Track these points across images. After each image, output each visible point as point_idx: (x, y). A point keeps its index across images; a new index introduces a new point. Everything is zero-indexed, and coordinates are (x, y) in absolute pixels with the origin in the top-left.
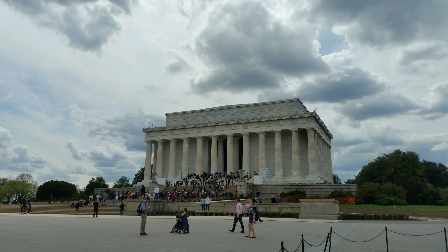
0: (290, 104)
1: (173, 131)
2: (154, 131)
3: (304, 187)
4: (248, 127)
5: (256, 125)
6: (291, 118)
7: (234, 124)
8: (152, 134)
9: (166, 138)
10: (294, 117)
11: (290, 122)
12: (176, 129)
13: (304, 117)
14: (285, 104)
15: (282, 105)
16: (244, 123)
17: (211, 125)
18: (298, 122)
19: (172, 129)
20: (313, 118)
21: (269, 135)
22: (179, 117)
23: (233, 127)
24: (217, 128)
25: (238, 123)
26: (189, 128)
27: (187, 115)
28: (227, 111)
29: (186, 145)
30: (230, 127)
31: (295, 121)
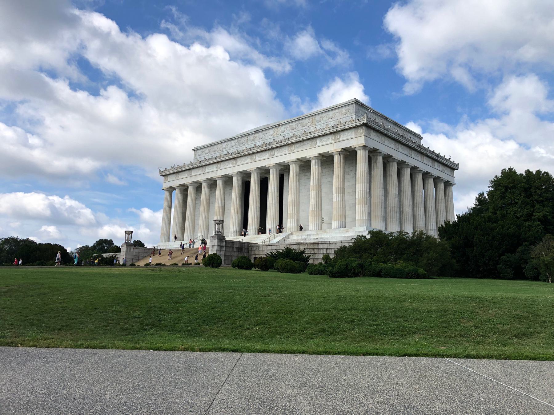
0: (343, 110)
1: (190, 172)
3: (316, 247)
4: (276, 154)
5: (286, 150)
6: (331, 133)
7: (259, 152)
8: (171, 178)
10: (334, 130)
11: (330, 139)
13: (350, 128)
14: (336, 111)
15: (331, 114)
16: (270, 149)
17: (232, 157)
18: (341, 139)
20: (364, 127)
21: (305, 165)
22: (207, 150)
24: (240, 161)
25: (263, 151)
26: (207, 165)
27: (215, 147)
29: (205, 190)
30: (254, 157)
31: (337, 136)
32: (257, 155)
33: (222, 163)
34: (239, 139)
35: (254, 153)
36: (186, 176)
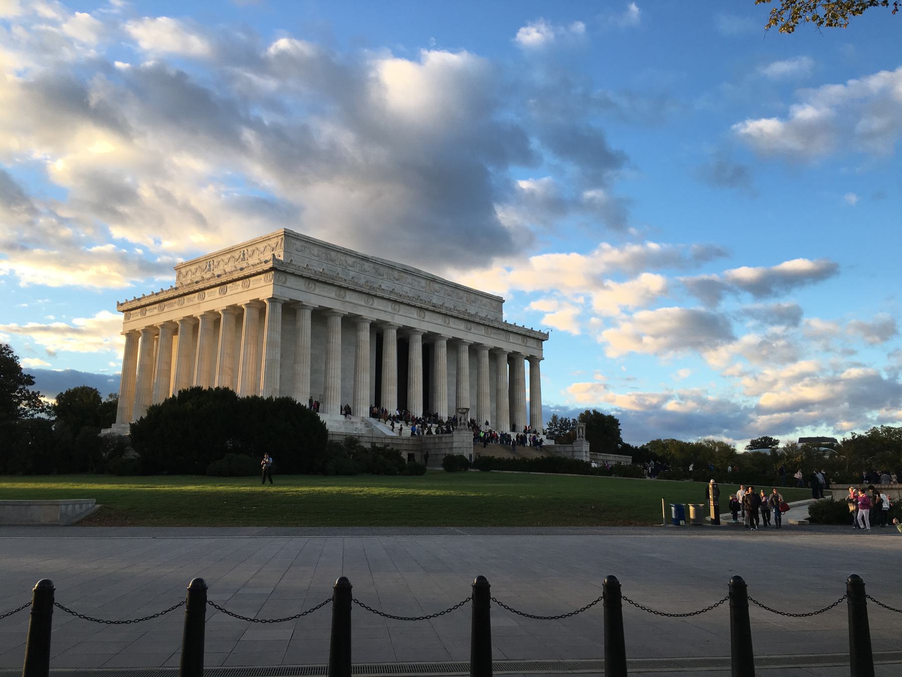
0: (495, 304)
1: (342, 292)
2: (301, 277)
4: (472, 330)
5: (482, 330)
9: (327, 304)
10: (528, 334)
11: (519, 340)
12: (354, 291)
15: (485, 301)
16: (469, 321)
19: (344, 284)
22: (316, 251)
23: (453, 323)
24: (428, 316)
26: (382, 298)
27: (333, 254)
28: (409, 279)
32: (451, 320)
33: (402, 306)
34: (377, 266)
35: (452, 316)
36: (333, 295)
